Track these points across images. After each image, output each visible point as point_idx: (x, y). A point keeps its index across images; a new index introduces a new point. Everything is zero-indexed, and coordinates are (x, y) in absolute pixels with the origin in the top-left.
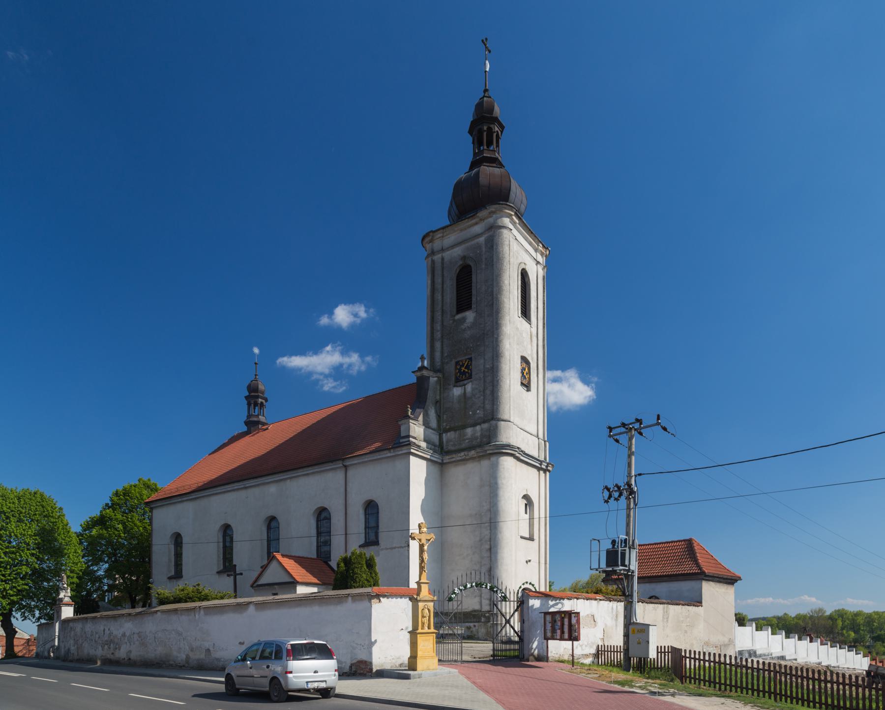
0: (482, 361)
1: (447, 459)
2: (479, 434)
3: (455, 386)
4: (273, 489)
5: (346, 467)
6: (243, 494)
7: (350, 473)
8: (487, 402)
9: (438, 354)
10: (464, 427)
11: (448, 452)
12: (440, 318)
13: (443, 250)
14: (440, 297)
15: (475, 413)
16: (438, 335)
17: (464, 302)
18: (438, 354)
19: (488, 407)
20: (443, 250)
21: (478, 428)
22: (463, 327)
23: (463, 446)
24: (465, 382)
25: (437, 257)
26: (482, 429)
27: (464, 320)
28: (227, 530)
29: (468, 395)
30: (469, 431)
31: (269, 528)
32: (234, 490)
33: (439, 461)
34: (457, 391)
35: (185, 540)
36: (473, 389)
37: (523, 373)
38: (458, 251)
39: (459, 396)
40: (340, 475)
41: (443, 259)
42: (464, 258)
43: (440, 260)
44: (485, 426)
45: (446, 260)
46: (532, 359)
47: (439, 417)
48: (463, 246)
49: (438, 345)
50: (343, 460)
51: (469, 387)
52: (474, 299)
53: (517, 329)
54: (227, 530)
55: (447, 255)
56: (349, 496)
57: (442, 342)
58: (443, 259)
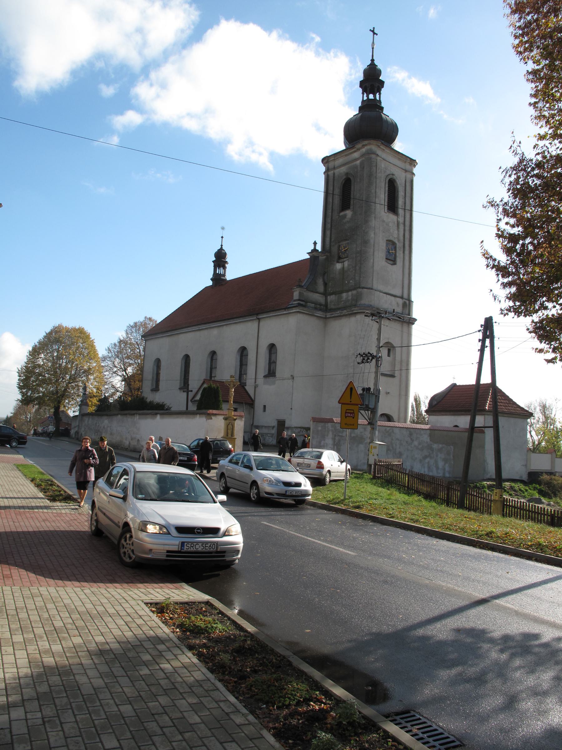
0: (355, 246)
1: (328, 315)
2: (350, 298)
3: (338, 262)
4: (215, 332)
5: (259, 319)
6: (198, 333)
7: (261, 324)
8: (357, 275)
9: (328, 239)
10: (342, 292)
11: (331, 310)
12: (330, 214)
13: (334, 168)
14: (331, 200)
15: (349, 282)
16: (329, 226)
17: (345, 204)
18: (328, 239)
19: (357, 278)
20: (334, 168)
21: (350, 293)
22: (344, 221)
23: (340, 306)
24: (345, 259)
25: (331, 173)
26: (352, 294)
27: (345, 216)
28: (187, 358)
29: (345, 269)
30: (344, 295)
31: (212, 359)
32: (193, 331)
33: (324, 316)
34: (339, 266)
35: (163, 364)
36: (349, 265)
37: (388, 252)
38: (343, 169)
39: (340, 270)
40: (255, 324)
41: (334, 174)
42: (347, 174)
43: (332, 175)
44: (354, 292)
45: (336, 175)
46: (399, 240)
47: (325, 284)
48: (347, 166)
49: (328, 233)
50: (257, 314)
51: (346, 264)
52: (352, 202)
53: (384, 221)
54: (187, 358)
55: (337, 171)
56: (260, 340)
57: (331, 231)
58: (334, 174)
